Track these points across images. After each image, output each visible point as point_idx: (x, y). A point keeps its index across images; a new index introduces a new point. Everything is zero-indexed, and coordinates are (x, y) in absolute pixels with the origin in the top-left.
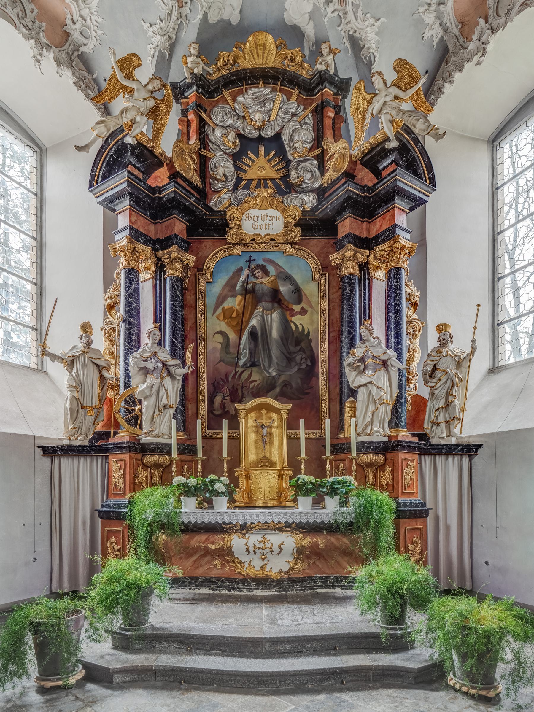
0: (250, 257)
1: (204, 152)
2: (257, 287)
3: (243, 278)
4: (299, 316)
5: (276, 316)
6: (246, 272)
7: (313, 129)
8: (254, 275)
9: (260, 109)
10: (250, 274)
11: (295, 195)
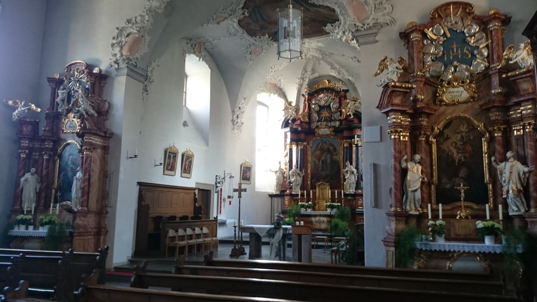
1: (310, 112)
5: (329, 156)
6: (321, 144)
8: (323, 145)
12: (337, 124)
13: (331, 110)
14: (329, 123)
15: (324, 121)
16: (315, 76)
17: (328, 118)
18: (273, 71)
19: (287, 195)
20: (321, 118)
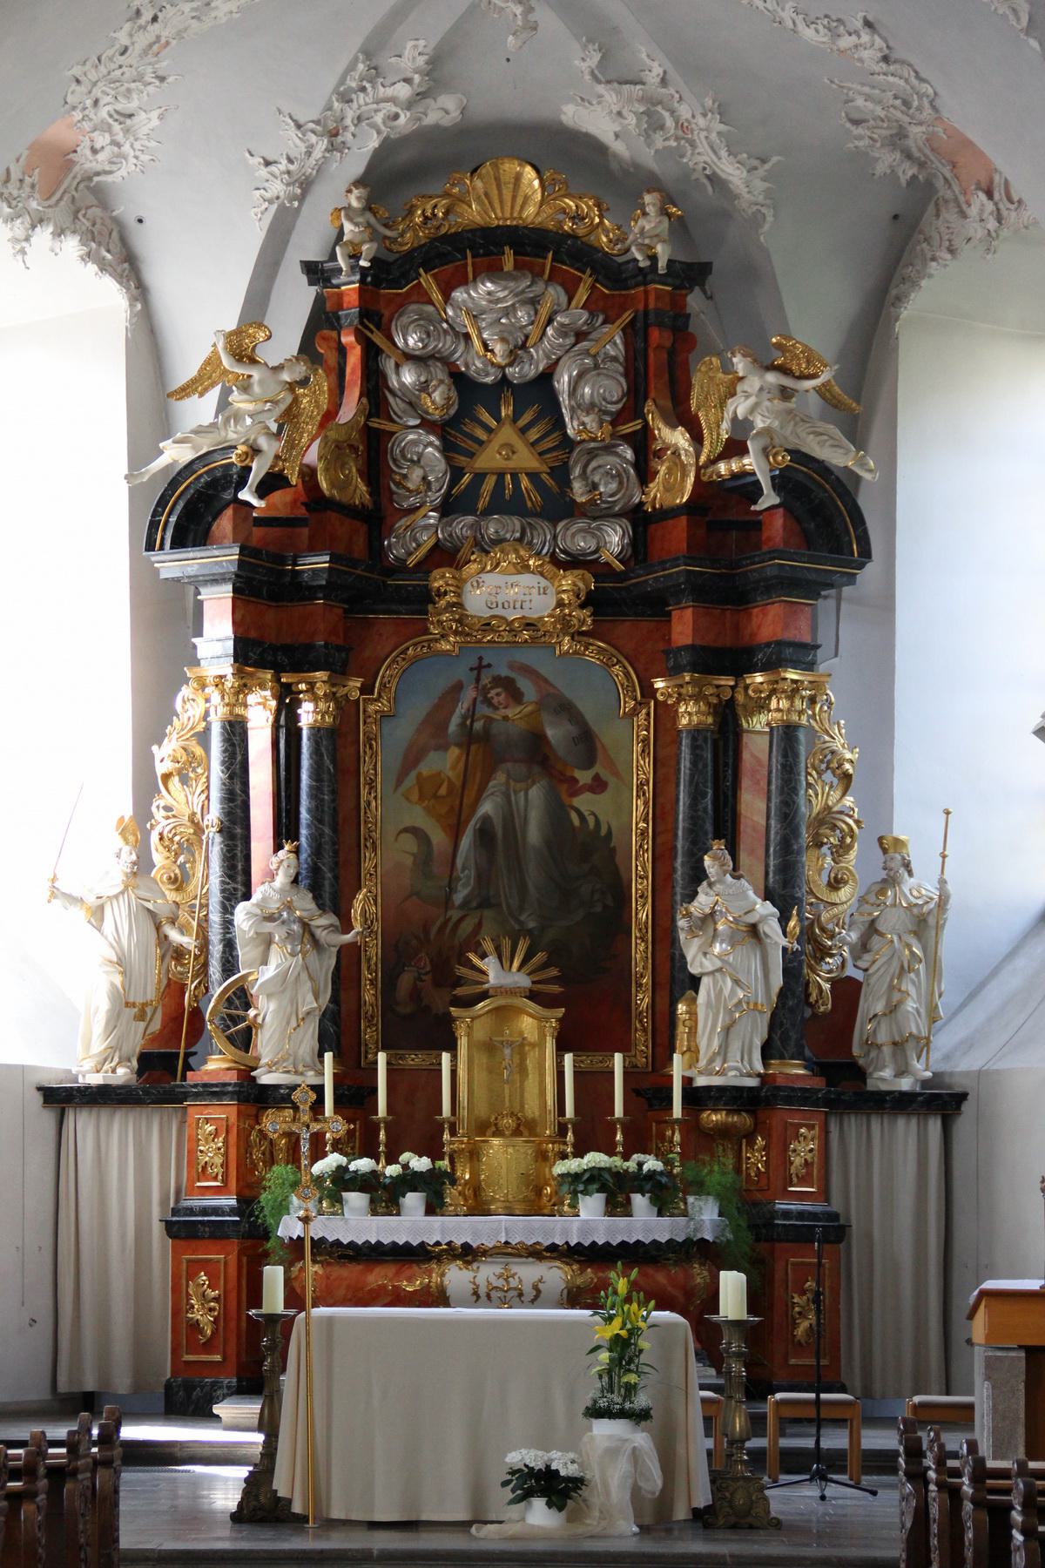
0: (481, 658)
1: (375, 423)
2: (495, 729)
3: (462, 708)
4: (587, 796)
5: (536, 794)
6: (469, 694)
7: (626, 369)
8: (488, 702)
9: (503, 321)
10: (480, 699)
11: (581, 524)
12: (615, 538)
13: (559, 424)
14: (546, 525)
15: (500, 505)
16: (432, 118)
17: (525, 483)
18: (142, 40)
19: (212, 1092)
20: (467, 478)
